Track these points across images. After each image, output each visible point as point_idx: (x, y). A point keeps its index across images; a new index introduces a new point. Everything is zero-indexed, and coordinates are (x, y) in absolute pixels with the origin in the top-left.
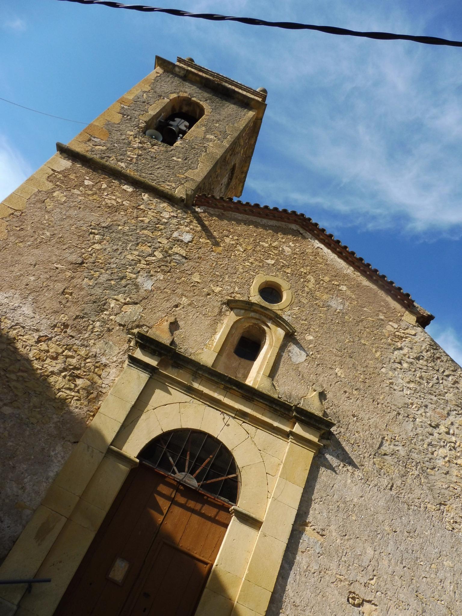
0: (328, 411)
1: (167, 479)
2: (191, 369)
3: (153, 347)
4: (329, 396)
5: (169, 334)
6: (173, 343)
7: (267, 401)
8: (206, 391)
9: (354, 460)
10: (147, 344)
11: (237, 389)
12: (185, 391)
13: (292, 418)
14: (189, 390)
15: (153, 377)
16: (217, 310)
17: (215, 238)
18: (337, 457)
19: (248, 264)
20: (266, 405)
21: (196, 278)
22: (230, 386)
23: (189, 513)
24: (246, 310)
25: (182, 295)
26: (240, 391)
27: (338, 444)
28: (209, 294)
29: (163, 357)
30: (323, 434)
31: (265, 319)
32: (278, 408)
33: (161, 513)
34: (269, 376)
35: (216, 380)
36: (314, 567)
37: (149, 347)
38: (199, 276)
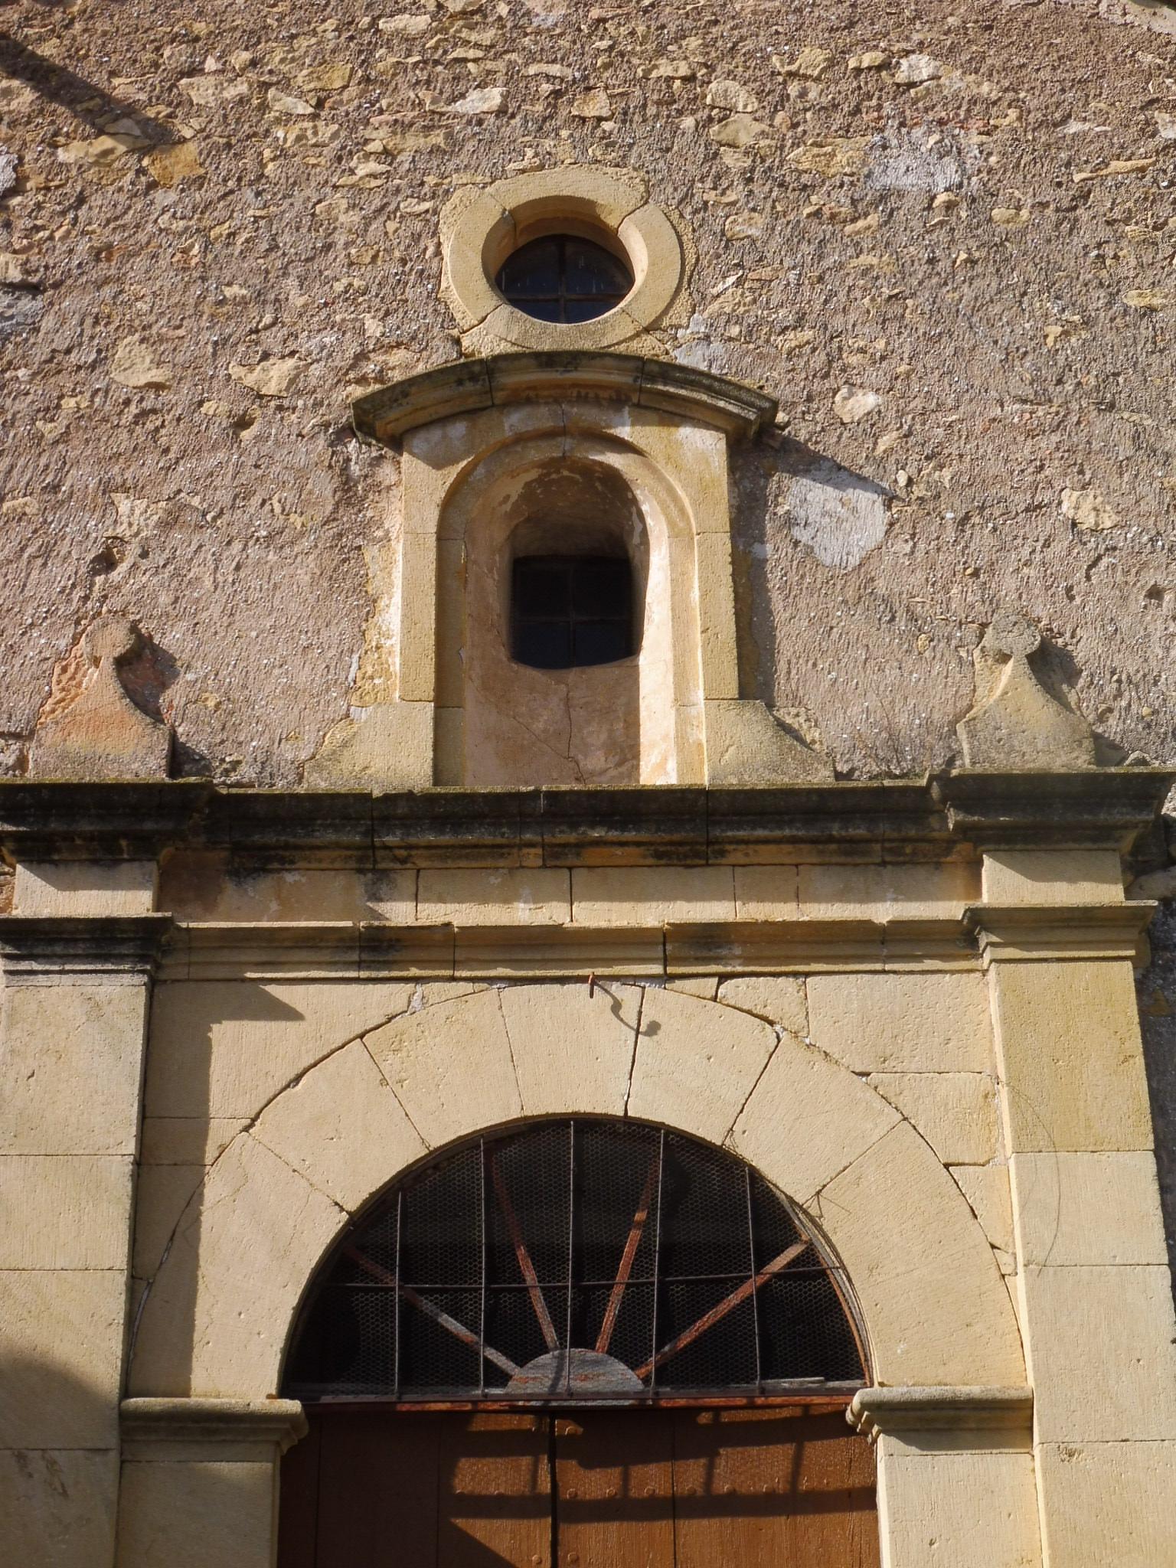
0: (1113, 728)
1: (479, 1425)
2: (338, 846)
3: (86, 827)
4: (1085, 649)
5: (137, 721)
6: (178, 756)
7: (790, 823)
8: (463, 915)
10: (54, 825)
11: (614, 835)
12: (359, 965)
13: (949, 844)
14: (379, 952)
15: (163, 976)
16: (324, 486)
17: (130, 110)
19: (373, 166)
20: (793, 840)
21: (135, 368)
22: (572, 837)
23: (661, 1528)
24: (470, 414)
25: (107, 488)
26: (631, 835)
28: (243, 423)
29: (165, 853)
30: (1137, 849)
31: (588, 415)
32: (861, 832)
34: (745, 693)
35: (488, 839)
37: (69, 837)
38: (144, 356)
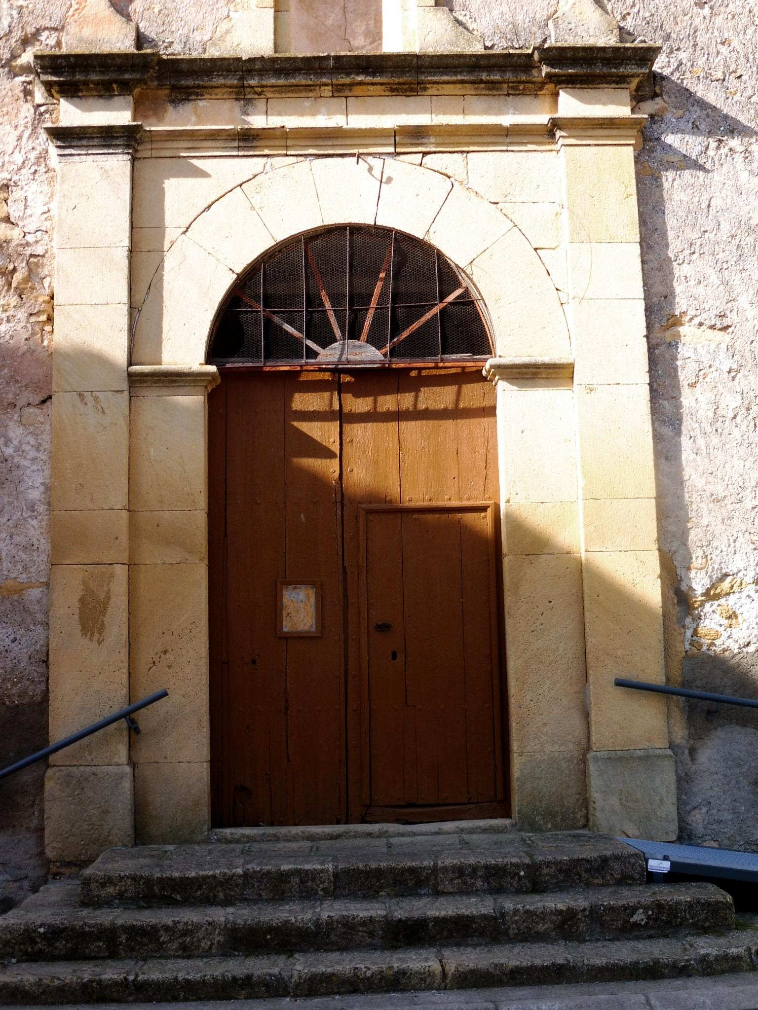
0: (629, 24)
1: (304, 377)
2: (225, 86)
3: (95, 77)
5: (118, 19)
6: (140, 40)
7: (461, 73)
8: (292, 122)
9: (741, 118)
10: (78, 77)
11: (369, 79)
12: (238, 148)
13: (543, 84)
14: (248, 140)
15: (138, 155)
18: (695, 129)
20: (462, 82)
22: (347, 80)
23: (394, 425)
26: (378, 79)
27: (687, 96)
29: (136, 91)
30: (638, 89)
32: (496, 77)
33: (328, 454)
35: (304, 82)
36: (731, 402)
37: (86, 83)
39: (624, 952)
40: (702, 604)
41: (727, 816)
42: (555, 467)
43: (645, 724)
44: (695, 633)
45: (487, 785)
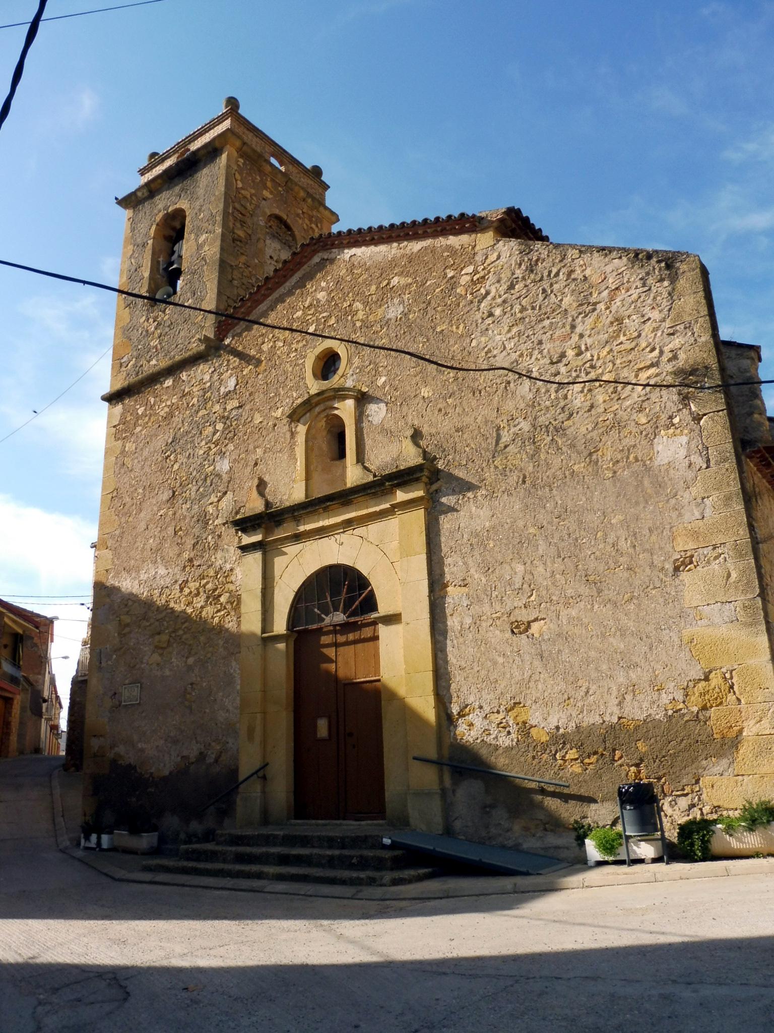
1: (325, 630)
4: (425, 430)
9: (473, 481)
14: (297, 538)
16: (288, 435)
17: (254, 357)
18: (454, 492)
19: (294, 354)
21: (258, 419)
23: (352, 646)
24: (309, 410)
25: (255, 448)
27: (451, 476)
28: (275, 425)
31: (329, 403)
33: (331, 661)
34: (358, 462)
36: (468, 621)
38: (259, 415)
39: (346, 874)
40: (458, 719)
41: (470, 824)
42: (398, 660)
43: (427, 777)
44: (455, 734)
45: (374, 805)
